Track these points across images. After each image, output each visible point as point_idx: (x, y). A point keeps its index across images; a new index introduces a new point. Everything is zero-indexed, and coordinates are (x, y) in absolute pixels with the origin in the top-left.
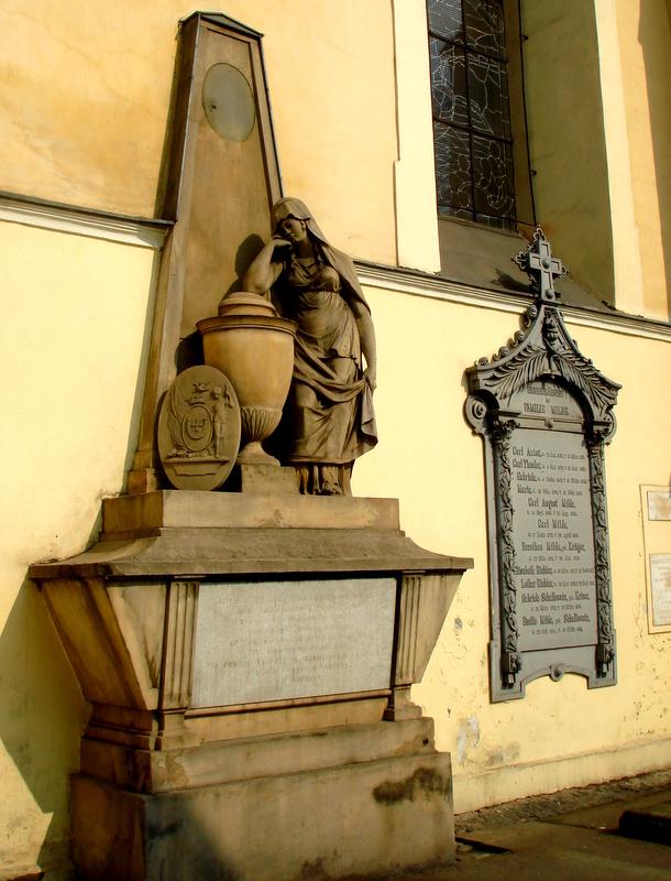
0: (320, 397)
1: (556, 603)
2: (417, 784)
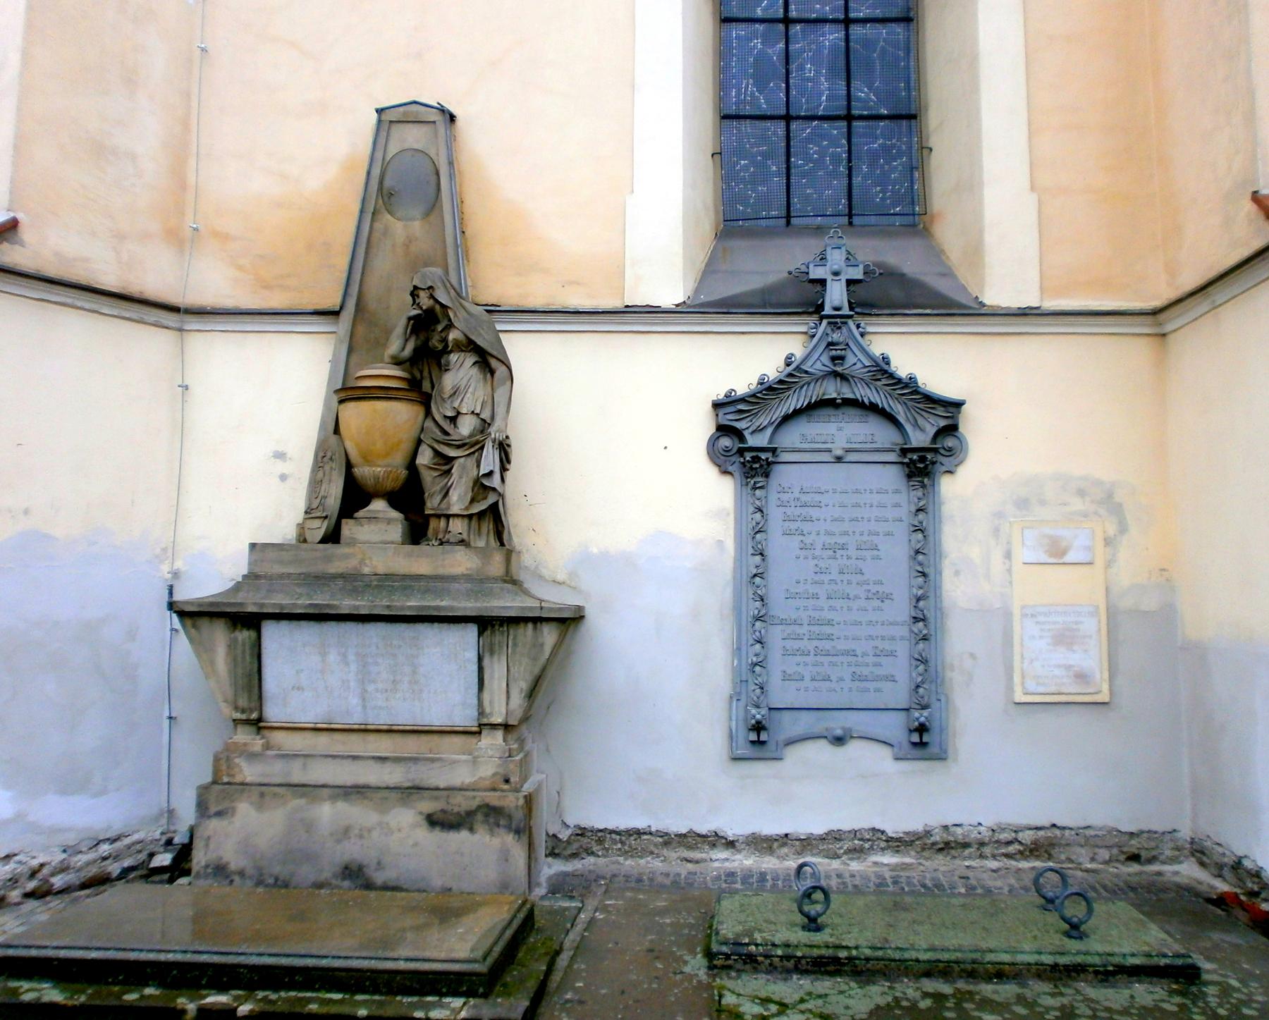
0: (437, 453)
1: (834, 659)
2: (479, 817)
